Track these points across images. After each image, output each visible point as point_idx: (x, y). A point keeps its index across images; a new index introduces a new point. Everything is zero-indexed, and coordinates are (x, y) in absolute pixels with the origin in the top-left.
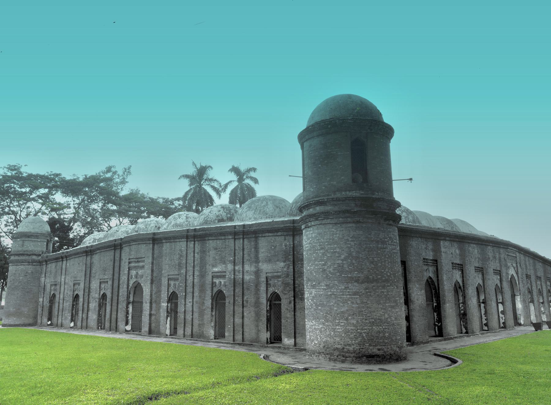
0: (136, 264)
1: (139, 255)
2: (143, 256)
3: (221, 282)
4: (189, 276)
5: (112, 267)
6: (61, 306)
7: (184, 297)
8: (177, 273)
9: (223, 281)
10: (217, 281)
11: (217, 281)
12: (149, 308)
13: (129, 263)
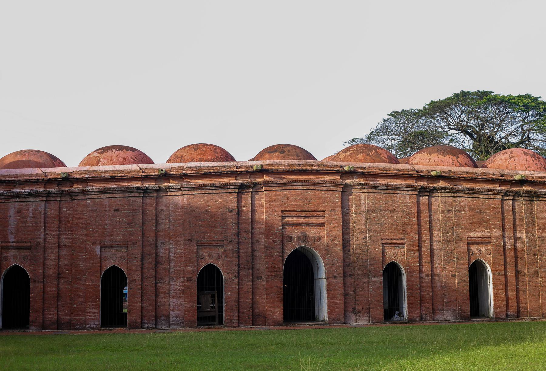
0: (302, 220)
1: (311, 207)
2: (322, 209)
3: (480, 251)
4: (425, 241)
5: (236, 222)
6: (51, 290)
7: (417, 269)
8: (401, 236)
9: (483, 249)
10: (475, 249)
11: (475, 249)
12: (342, 285)
13: (283, 217)
